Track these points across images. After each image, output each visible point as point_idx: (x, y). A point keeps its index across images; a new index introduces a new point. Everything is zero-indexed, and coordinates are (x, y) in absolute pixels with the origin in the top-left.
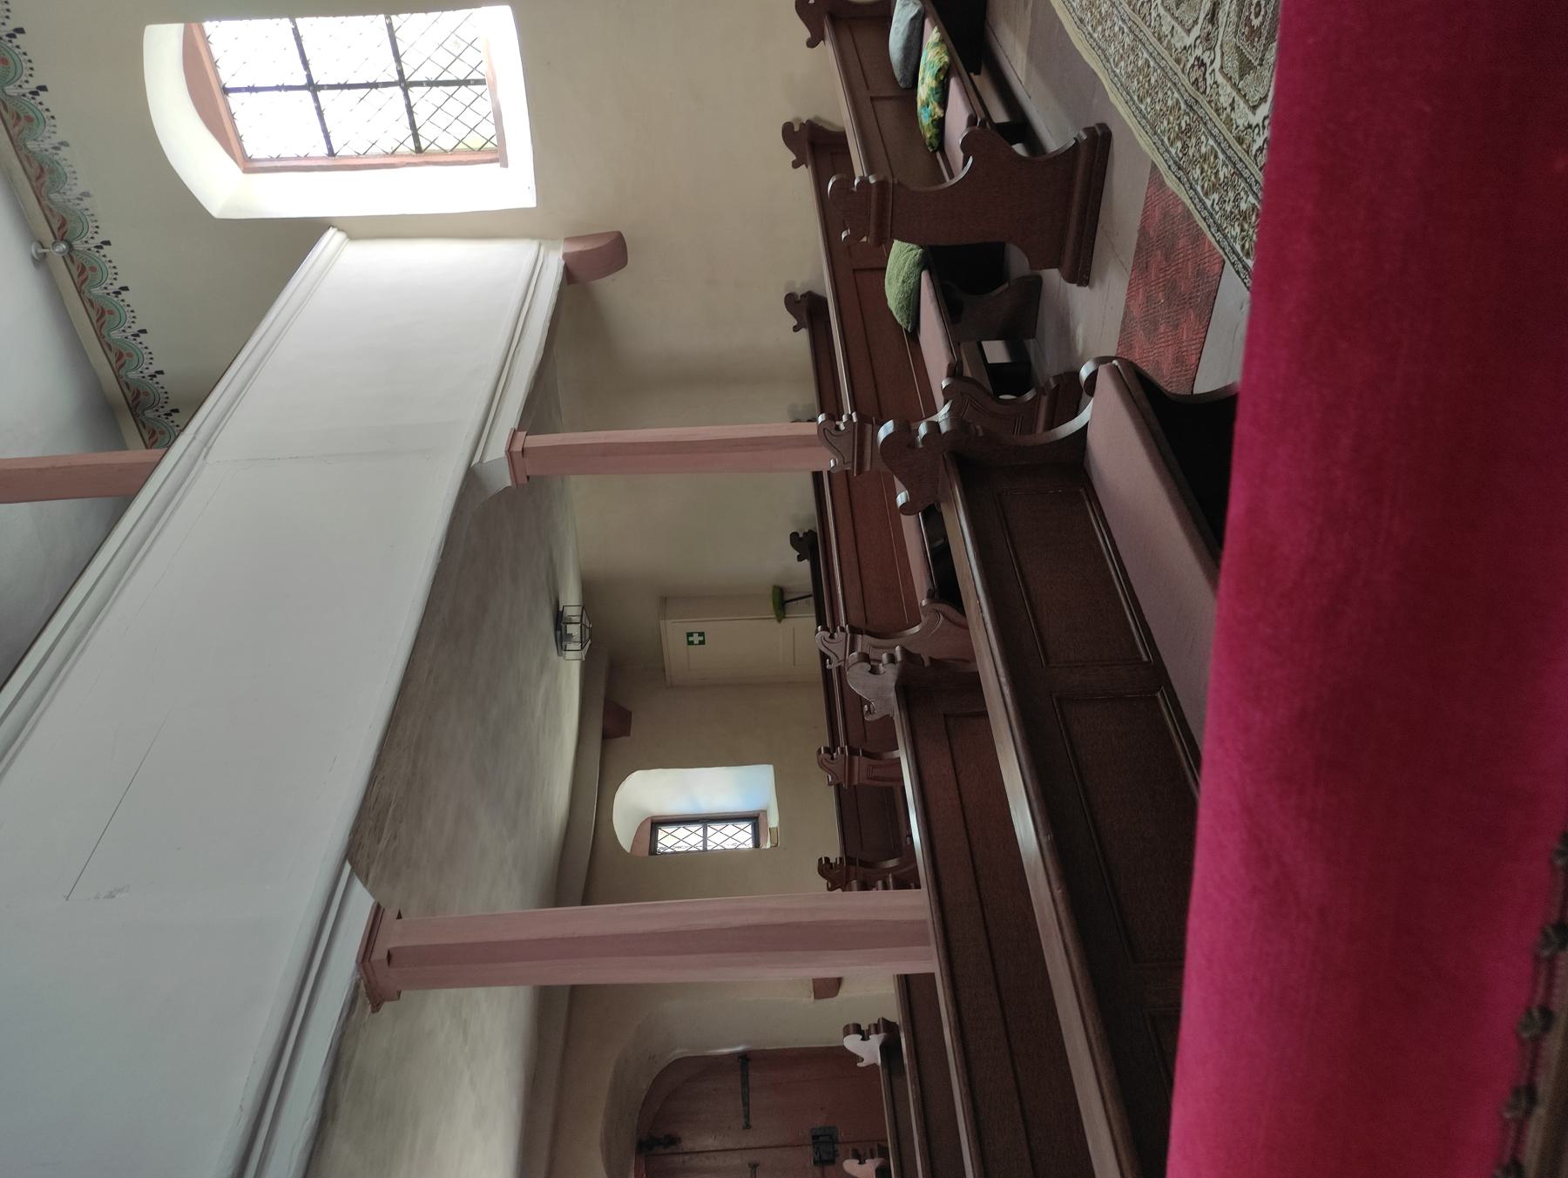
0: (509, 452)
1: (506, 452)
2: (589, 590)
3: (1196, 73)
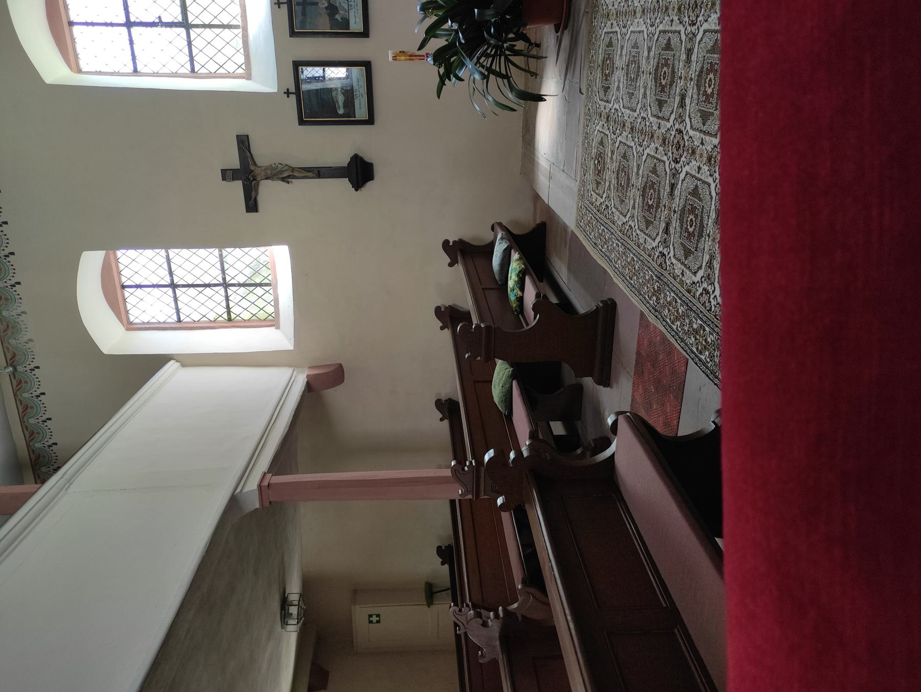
0: (260, 486)
1: (257, 486)
2: (307, 584)
3: (661, 260)
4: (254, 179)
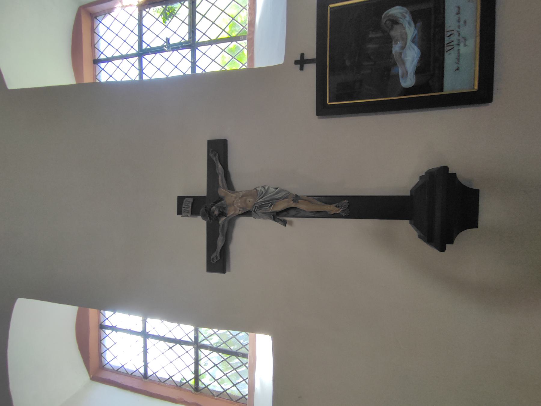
4: (223, 214)
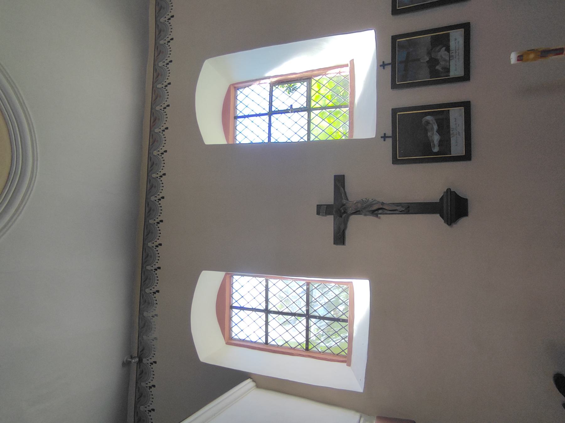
4: (345, 212)
